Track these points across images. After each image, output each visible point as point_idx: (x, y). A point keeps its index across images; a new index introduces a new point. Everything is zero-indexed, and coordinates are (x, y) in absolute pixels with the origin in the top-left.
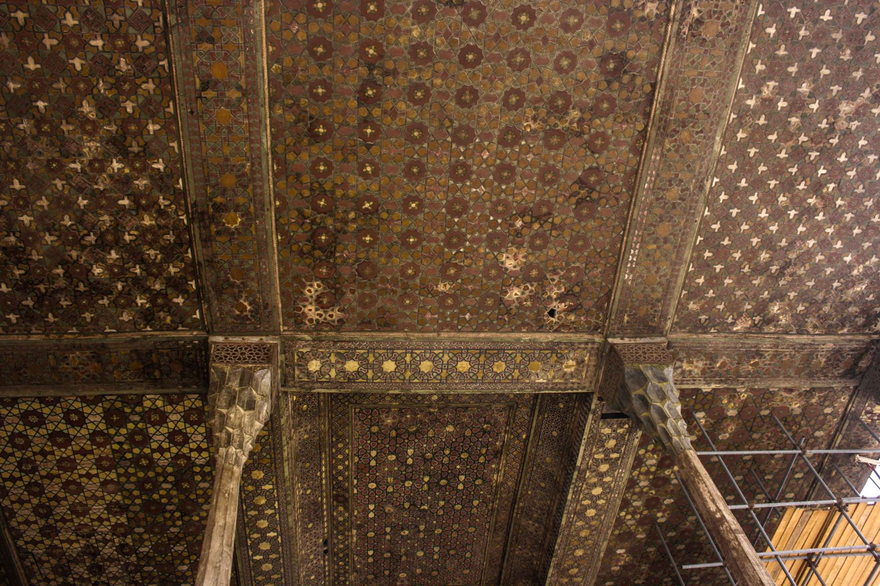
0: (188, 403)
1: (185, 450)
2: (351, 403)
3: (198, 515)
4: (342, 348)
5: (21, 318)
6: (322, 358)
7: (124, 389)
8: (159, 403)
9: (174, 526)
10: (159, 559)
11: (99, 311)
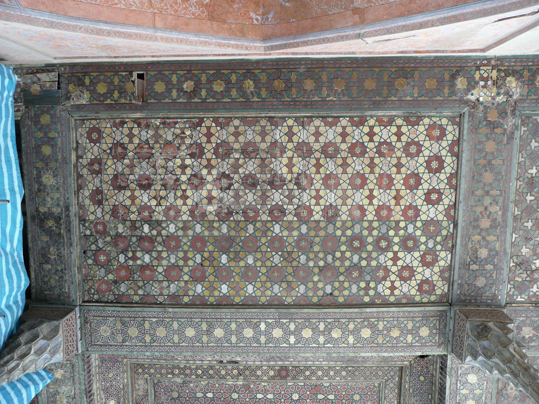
0: (440, 284)
1: (393, 277)
2: (386, 381)
4: (486, 397)
5: (532, 177)
6: (478, 384)
7: (462, 241)
8: (442, 263)
9: (308, 259)
10: (264, 240)
11: (532, 233)
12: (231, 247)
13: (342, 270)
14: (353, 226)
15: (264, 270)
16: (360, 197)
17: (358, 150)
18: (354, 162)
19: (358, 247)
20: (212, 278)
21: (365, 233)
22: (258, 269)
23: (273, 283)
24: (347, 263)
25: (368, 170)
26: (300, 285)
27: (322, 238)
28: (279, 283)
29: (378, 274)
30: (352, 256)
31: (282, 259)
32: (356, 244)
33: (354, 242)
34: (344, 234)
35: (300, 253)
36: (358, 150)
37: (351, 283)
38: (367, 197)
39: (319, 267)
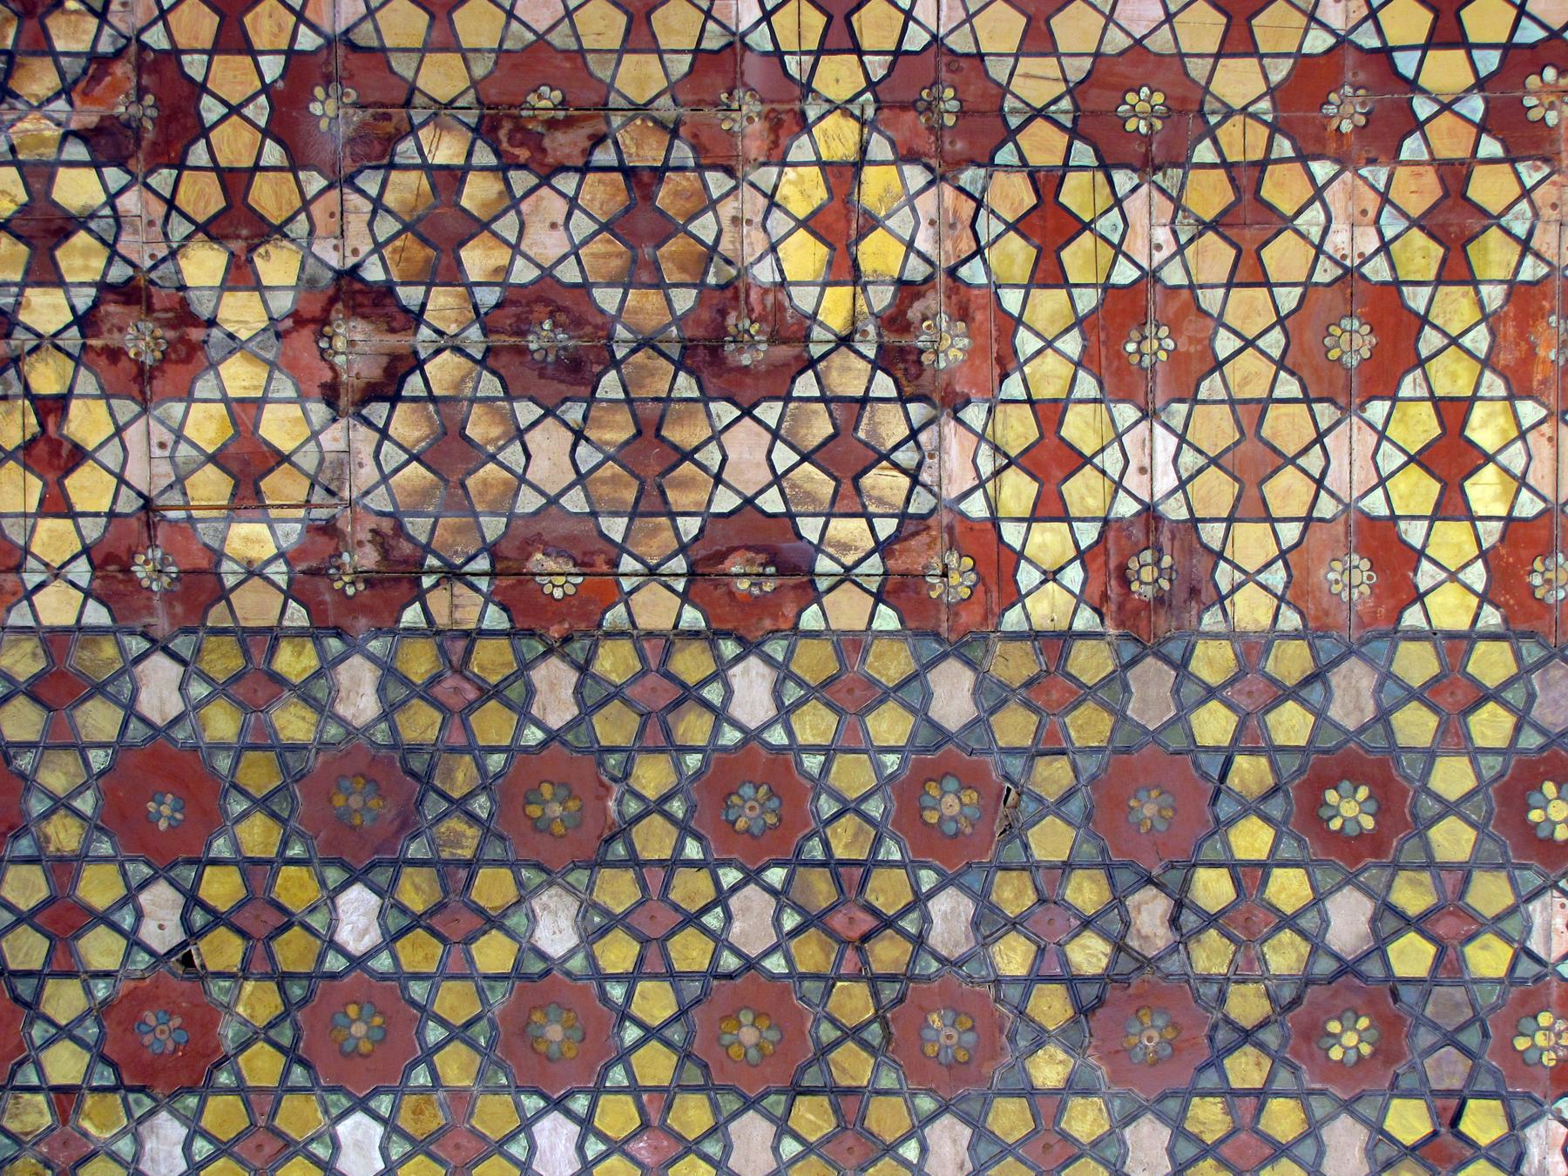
3: (1075, 1087)
9: (990, 923)
10: (652, 776)
12: (408, 825)
13: (1246, 1005)
14: (1317, 676)
15: (655, 1002)
16: (1369, 459)
17: (1346, 111)
18: (1318, 194)
19: (1362, 835)
20: (262, 1066)
21: (1416, 725)
22: (617, 992)
23: (730, 1103)
24: (1285, 956)
25: (1421, 255)
26: (933, 1118)
27: (1089, 765)
28: (776, 1103)
29: (1521, 1044)
30: (1318, 900)
31: (790, 921)
32: (1349, 809)
33: (1331, 796)
34: (1250, 737)
35: (928, 879)
36: (1346, 111)
37: (1320, 1107)
38: (1421, 459)
39: (1072, 981)
